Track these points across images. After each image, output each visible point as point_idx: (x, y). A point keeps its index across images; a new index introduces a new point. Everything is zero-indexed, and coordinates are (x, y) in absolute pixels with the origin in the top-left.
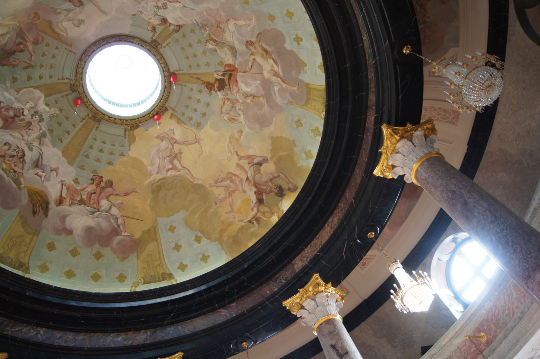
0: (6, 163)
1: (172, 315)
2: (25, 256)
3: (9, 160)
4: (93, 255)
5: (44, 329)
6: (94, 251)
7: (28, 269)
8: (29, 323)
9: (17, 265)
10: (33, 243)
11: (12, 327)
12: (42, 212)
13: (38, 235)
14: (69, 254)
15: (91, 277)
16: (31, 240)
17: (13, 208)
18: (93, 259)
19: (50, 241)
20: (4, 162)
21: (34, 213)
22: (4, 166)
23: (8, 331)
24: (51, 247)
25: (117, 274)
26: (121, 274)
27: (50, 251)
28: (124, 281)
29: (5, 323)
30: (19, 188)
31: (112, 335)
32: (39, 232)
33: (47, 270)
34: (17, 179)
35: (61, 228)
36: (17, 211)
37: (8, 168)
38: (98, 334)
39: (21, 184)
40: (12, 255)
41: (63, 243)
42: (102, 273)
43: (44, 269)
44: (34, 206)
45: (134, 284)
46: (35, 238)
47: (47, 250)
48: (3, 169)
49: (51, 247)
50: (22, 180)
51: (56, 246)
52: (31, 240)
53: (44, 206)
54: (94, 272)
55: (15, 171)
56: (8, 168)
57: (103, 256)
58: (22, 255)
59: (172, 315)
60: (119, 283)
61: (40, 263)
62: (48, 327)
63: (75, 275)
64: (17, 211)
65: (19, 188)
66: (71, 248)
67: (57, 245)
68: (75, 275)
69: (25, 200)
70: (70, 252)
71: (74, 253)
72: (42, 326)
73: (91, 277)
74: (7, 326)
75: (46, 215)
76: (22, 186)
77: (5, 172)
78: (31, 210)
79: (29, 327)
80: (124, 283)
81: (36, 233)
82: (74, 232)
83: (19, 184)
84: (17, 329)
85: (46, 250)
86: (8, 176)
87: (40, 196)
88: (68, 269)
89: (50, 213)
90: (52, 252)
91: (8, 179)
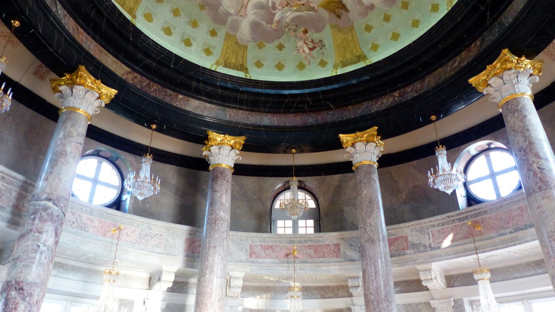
0: (293, 6)
1: (488, 13)
2: (357, 49)
3: (293, 3)
4: (402, 8)
5: (398, 92)
6: (400, 4)
7: (365, 56)
8: (385, 94)
9: (356, 59)
10: (355, 37)
11: (375, 104)
12: (343, 12)
13: (354, 28)
14: (384, 23)
15: (412, 26)
16: (352, 36)
17: (324, 27)
18: (403, 11)
19: (365, 26)
20: (292, 6)
21: (339, 16)
22: (294, 8)
23: (374, 109)
24: (368, 28)
25: (430, 8)
26: (432, 5)
27: (370, 32)
28: (438, 9)
29: (370, 104)
30: (316, 11)
31: (450, 64)
32: (353, 26)
33: (378, 46)
34: (309, 8)
35: (364, 10)
36: (328, 27)
37: (298, 7)
38: (438, 70)
39: (314, 8)
40: (348, 56)
41: (374, 19)
42: (418, 17)
43: (375, 48)
44: (334, 12)
45: (447, 5)
46: (353, 32)
47: (367, 33)
48: (296, 11)
49: (368, 28)
50: (312, 5)
51: (371, 25)
52: (352, 36)
53: (340, 6)
54: (411, 21)
55: (303, 5)
56: (298, 7)
57: (408, 3)
58: (355, 51)
59: (488, 13)
60: (436, 14)
61: (370, 46)
62: (399, 89)
63: (399, 35)
64: (328, 27)
65: (316, 11)
66: (382, 17)
67: (371, 24)
68: (399, 35)
69: (325, 14)
70: (383, 20)
71: (387, 19)
72: (395, 91)
73: (412, 26)
74: (372, 105)
75: (347, 10)
76: (316, 8)
77: (299, 11)
78: (335, 17)
79: (387, 97)
80: (439, 11)
81: (352, 28)
82: (375, 4)
83: (312, 9)
84: (379, 103)
85: (367, 35)
86: (302, 12)
87: (332, 3)
88: (391, 34)
89: (348, 7)
90: (372, 32)
91: (304, 13)
